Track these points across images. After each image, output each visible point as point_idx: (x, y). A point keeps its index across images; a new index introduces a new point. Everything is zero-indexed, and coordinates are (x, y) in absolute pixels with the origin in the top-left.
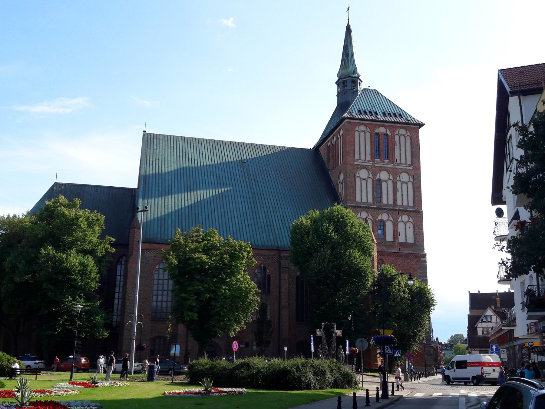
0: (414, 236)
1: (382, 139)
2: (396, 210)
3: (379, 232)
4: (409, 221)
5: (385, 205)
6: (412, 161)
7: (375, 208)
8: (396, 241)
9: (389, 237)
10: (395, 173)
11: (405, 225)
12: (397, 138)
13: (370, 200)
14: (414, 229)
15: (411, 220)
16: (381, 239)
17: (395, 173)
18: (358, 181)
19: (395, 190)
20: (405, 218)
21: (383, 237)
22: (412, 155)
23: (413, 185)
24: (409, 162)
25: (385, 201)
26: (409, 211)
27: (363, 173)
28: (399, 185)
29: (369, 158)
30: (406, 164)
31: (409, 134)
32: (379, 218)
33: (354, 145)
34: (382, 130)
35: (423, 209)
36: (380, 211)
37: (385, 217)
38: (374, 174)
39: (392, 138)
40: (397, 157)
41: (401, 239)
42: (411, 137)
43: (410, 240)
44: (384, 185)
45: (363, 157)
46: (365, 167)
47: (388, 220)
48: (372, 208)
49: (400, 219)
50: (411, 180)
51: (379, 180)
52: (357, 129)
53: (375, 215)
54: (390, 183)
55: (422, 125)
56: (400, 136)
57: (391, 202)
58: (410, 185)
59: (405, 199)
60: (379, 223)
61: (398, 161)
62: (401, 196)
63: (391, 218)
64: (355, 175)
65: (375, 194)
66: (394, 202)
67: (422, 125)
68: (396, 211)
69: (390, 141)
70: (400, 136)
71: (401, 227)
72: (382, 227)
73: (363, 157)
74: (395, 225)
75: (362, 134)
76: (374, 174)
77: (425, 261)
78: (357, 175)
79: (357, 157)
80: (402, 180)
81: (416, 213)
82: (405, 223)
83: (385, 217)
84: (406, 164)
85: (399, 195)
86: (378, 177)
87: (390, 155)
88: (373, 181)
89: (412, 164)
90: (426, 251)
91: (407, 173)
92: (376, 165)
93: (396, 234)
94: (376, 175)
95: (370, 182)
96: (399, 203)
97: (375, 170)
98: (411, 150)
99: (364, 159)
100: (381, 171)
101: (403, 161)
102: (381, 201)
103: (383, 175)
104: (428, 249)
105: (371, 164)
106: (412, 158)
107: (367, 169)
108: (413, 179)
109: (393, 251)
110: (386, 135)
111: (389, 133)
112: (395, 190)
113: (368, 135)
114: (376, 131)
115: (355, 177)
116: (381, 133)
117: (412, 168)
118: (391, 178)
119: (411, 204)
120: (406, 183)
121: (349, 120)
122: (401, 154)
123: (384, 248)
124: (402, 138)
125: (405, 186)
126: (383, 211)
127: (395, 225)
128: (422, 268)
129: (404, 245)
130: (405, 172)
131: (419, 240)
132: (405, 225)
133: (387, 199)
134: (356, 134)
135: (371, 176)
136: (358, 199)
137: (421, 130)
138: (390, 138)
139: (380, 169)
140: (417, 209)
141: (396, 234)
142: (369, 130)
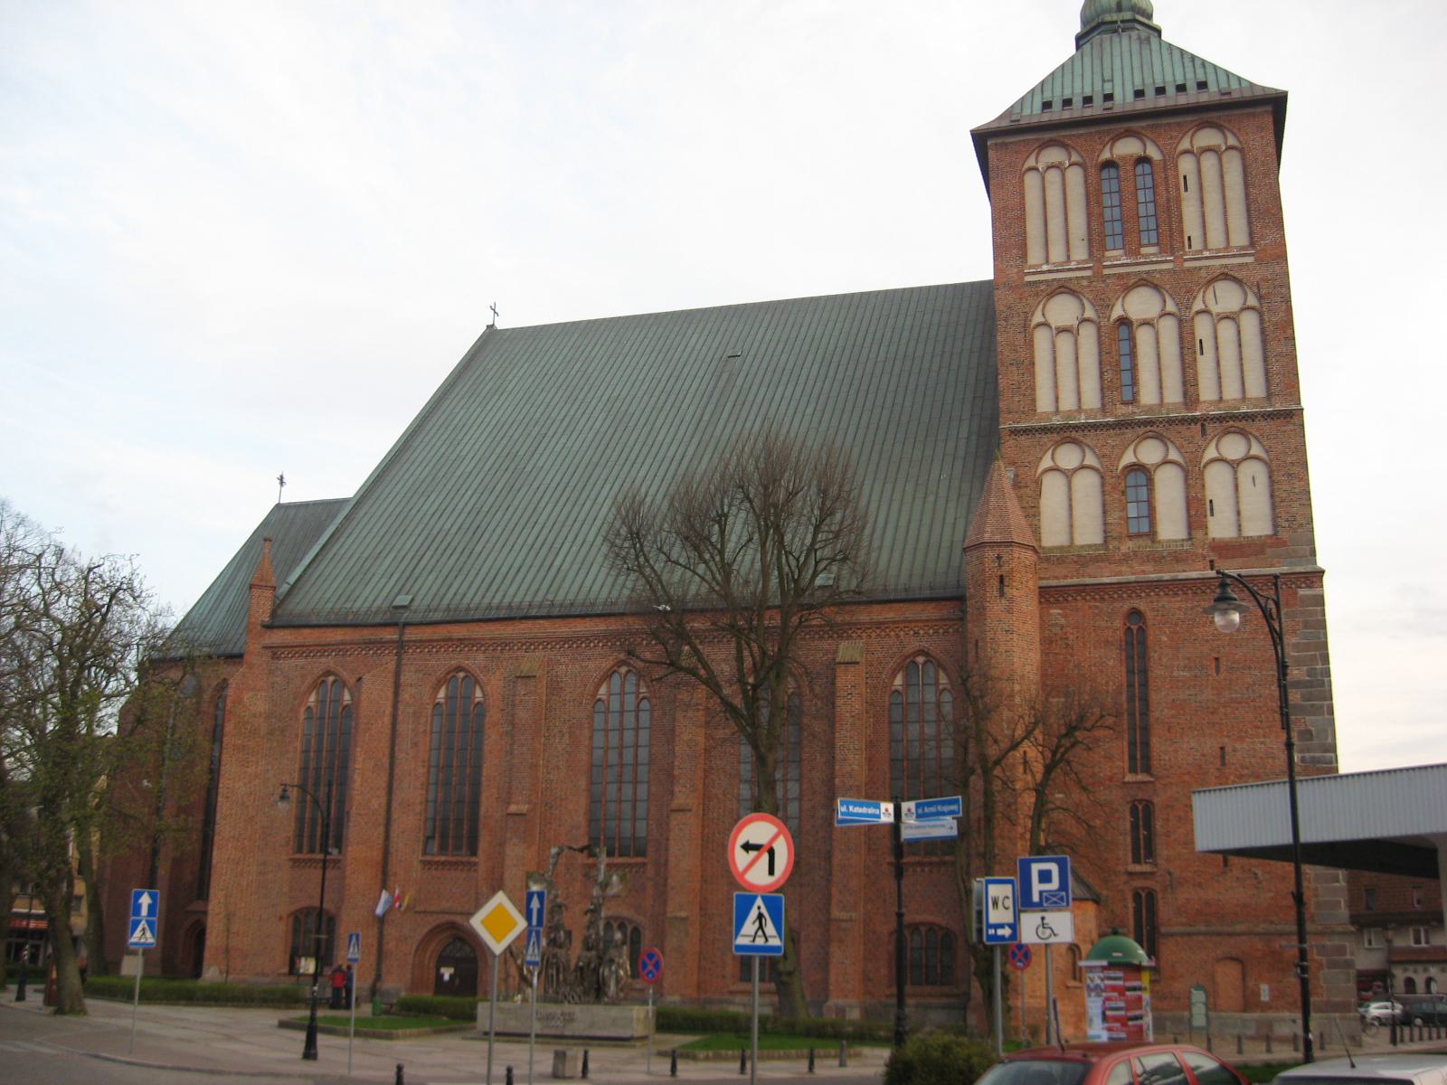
0: (1274, 507)
2: (1194, 420)
3: (1132, 511)
4: (1248, 458)
5: (1150, 409)
6: (1251, 234)
7: (1108, 426)
8: (1198, 534)
9: (1171, 527)
10: (1182, 288)
12: (1186, 165)
13: (1092, 399)
14: (1272, 481)
15: (1256, 450)
16: (1139, 535)
17: (1182, 288)
18: (1041, 339)
19: (1188, 348)
20: (1233, 447)
21: (1145, 528)
23: (1262, 321)
24: (1240, 238)
25: (1148, 396)
26: (1246, 417)
27: (1062, 310)
28: (1202, 328)
29: (1080, 253)
31: (1232, 141)
32: (1128, 458)
34: (1128, 148)
35: (1304, 404)
36: (1129, 433)
37: (1150, 452)
40: (1191, 226)
41: (1220, 527)
42: (1241, 151)
43: (1258, 525)
44: (1144, 337)
45: (1057, 254)
46: (1064, 288)
47: (1166, 462)
48: (1095, 427)
49: (1211, 453)
50: (1252, 301)
51: (1124, 321)
52: (1031, 162)
53: (1107, 451)
54: (1168, 328)
56: (1198, 154)
57: (1173, 395)
58: (1250, 323)
59: (1231, 376)
60: (1131, 480)
61: (1197, 245)
62: (1213, 365)
63: (1174, 455)
64: (1026, 321)
65: (1107, 376)
66: (1185, 394)
68: (1192, 426)
69: (1160, 177)
70: (1198, 154)
71: (1217, 483)
72: (1143, 493)
73: (1057, 254)
76: (1104, 305)
77: (1320, 601)
78: (1038, 318)
79: (1035, 256)
80: (1215, 309)
81: (1276, 422)
82: (1234, 465)
85: (1205, 364)
86: (1117, 312)
89: (1252, 244)
90: (1321, 562)
92: (1106, 272)
93: (1197, 510)
94: (1110, 307)
95: (1088, 335)
96: (1207, 392)
99: (1062, 258)
100: (1128, 289)
101: (1216, 240)
102: (1134, 400)
103: (1140, 304)
104: (1329, 550)
105: (1088, 273)
107: (1073, 292)
108: (1260, 298)
109: (1182, 575)
110: (1144, 160)
111: (1153, 153)
112: (1188, 348)
114: (1106, 155)
115: (1027, 330)
116: (1123, 158)
117: (1249, 260)
118: (1171, 307)
119: (1256, 388)
120: (1232, 317)
121: (1000, 140)
122: (1210, 216)
123: (1149, 567)
125: (1226, 330)
126: (1141, 431)
128: (1306, 625)
129: (1239, 548)
130: (1225, 276)
131: (1292, 519)
133: (1156, 386)
134: (1031, 181)
135: (1090, 313)
136: (1044, 403)
139: (1128, 285)
140: (1278, 407)
141: (1197, 510)
142: (1075, 158)
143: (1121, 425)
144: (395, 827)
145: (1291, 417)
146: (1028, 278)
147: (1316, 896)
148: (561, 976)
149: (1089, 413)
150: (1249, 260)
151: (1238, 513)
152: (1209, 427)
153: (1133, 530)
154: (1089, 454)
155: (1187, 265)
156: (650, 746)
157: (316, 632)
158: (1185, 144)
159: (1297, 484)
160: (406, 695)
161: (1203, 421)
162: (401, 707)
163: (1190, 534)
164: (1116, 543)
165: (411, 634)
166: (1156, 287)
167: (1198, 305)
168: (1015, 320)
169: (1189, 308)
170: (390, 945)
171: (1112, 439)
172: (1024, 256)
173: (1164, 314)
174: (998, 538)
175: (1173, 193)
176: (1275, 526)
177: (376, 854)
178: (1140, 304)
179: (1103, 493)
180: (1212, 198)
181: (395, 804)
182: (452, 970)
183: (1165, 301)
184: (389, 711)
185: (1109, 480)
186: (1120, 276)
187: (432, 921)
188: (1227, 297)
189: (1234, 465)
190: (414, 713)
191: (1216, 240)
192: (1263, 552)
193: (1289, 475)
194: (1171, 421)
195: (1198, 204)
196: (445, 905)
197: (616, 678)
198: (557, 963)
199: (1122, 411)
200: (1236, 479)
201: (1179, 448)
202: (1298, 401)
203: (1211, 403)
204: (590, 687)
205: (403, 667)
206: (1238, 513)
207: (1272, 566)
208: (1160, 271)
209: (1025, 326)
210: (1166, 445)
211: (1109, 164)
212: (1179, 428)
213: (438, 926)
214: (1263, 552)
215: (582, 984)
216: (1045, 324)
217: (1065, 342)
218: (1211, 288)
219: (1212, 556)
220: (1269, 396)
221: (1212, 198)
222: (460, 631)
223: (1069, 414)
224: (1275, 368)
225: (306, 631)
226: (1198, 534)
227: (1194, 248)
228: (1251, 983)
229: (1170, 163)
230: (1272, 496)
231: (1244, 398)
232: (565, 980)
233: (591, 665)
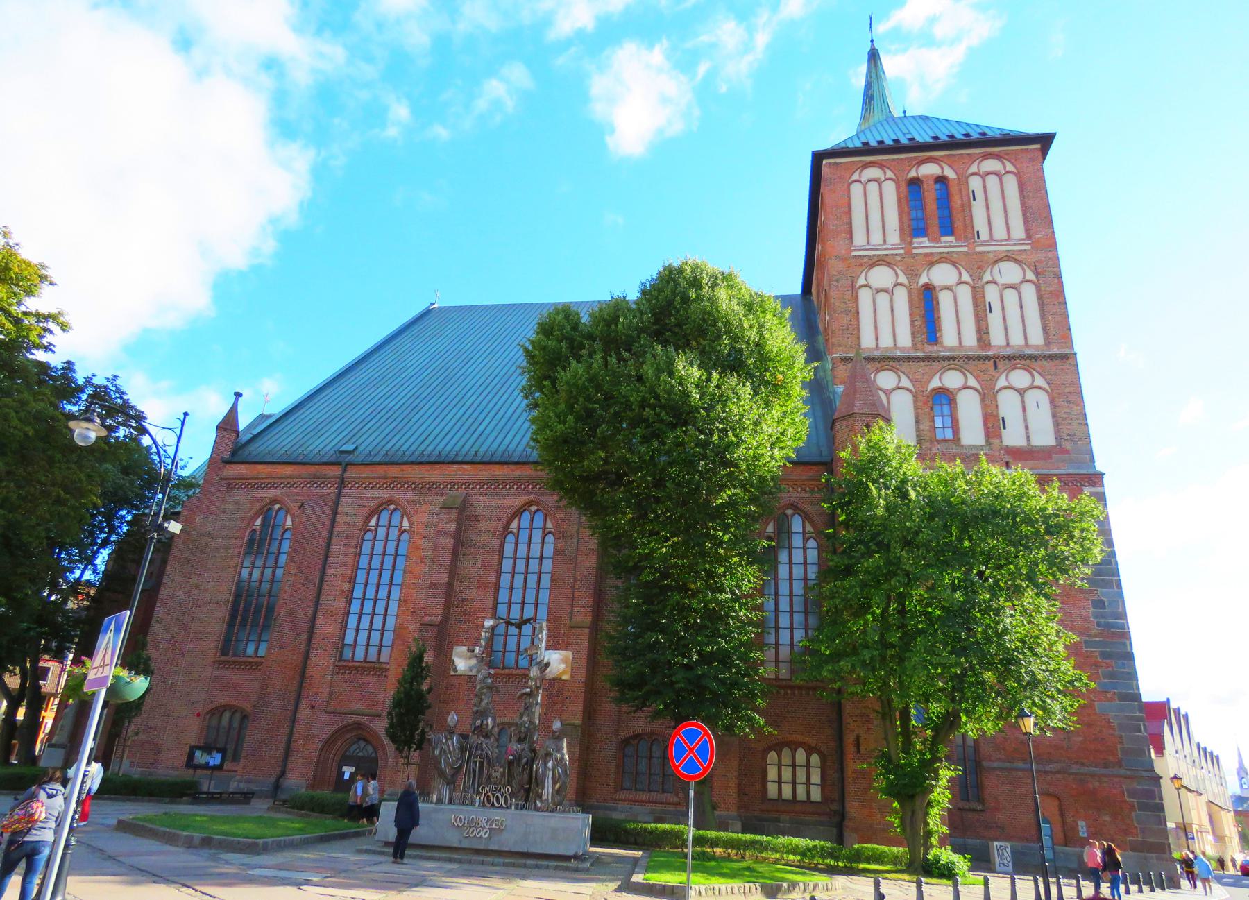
0: (1056, 424)
1: (931, 193)
2: (988, 358)
4: (1032, 387)
5: (952, 349)
6: (1027, 230)
8: (995, 442)
10: (977, 265)
11: (1022, 397)
12: (975, 183)
16: (946, 440)
17: (977, 265)
18: (865, 297)
19: (981, 309)
20: (1020, 378)
21: (949, 434)
22: (1024, 214)
23: (1038, 290)
24: (1018, 231)
25: (949, 338)
26: (1030, 357)
27: (881, 276)
28: (991, 294)
29: (894, 238)
30: (1009, 238)
32: (935, 383)
33: (849, 213)
35: (1077, 348)
36: (936, 365)
37: (952, 379)
38: (913, 274)
39: (959, 184)
40: (980, 224)
42: (1018, 175)
43: (1044, 436)
44: (945, 300)
45: (876, 239)
47: (965, 387)
48: (908, 359)
49: (1002, 382)
50: (1030, 275)
51: (929, 290)
52: (856, 176)
53: (918, 376)
54: (965, 294)
55: (1044, 141)
56: (984, 176)
57: (970, 339)
58: (1029, 293)
61: (984, 236)
66: (979, 339)
67: (1044, 141)
68: (988, 362)
70: (984, 176)
71: (1008, 405)
72: (946, 410)
73: (876, 239)
74: (988, 398)
75: (873, 187)
76: (913, 274)
78: (861, 281)
79: (859, 239)
80: (1001, 281)
81: (1055, 362)
82: (1021, 392)
83: (952, 379)
84: (1009, 238)
85: (994, 320)
86: (923, 280)
87: (958, 224)
88: (910, 292)
89: (1029, 237)
90: (1099, 466)
91: (1016, 261)
92: (915, 251)
94: (918, 276)
95: (901, 296)
96: (997, 338)
97: (911, 264)
98: (1023, 204)
100: (932, 264)
101: (1000, 233)
103: (941, 275)
105: (902, 252)
106: (1026, 222)
107: (889, 264)
108: (1037, 274)
111: (950, 173)
112: (981, 309)
113: (890, 189)
114: (913, 174)
115: (854, 289)
116: (927, 176)
117: (1029, 247)
118: (966, 277)
119: (1036, 338)
121: (832, 161)
124: (992, 181)
125: (1010, 296)
126: (946, 363)
127: (988, 398)
130: (1008, 257)
132: (1022, 397)
134: (856, 190)
135: (902, 279)
136: (867, 341)
137: (1053, 165)
138: (954, 189)
139: (931, 261)
140: (1055, 351)
143: (929, 359)
144: (318, 634)
145: (1067, 359)
146: (854, 254)
147: (1122, 743)
148: (485, 772)
149: (903, 349)
150: (1029, 247)
151: (1027, 428)
152: (1000, 364)
153: (939, 436)
154: (903, 377)
155: (978, 249)
156: (553, 572)
157: (269, 468)
158: (974, 169)
159: (1075, 408)
160: (341, 522)
161: (995, 360)
162: (336, 532)
163: (987, 441)
164: (928, 445)
165: (352, 472)
166: (954, 264)
167: (987, 277)
168: (844, 282)
169: (980, 278)
170: (298, 743)
171: (922, 367)
172: (851, 238)
173: (960, 283)
174: (866, 410)
175: (965, 201)
176: (1058, 438)
177: (297, 659)
178: (941, 275)
179: (916, 408)
180: (996, 205)
181: (320, 614)
182: (353, 769)
183: (960, 274)
184: (324, 533)
185: (920, 398)
186: (926, 255)
187: (339, 722)
188: (1010, 272)
189: (1021, 392)
190: (347, 537)
191: (1000, 233)
192: (1050, 458)
193: (1068, 401)
194: (969, 358)
195: (984, 209)
196: (354, 707)
197: (526, 516)
198: (481, 756)
199: (932, 350)
200: (1023, 402)
201: (977, 378)
202: (1072, 348)
203: (1000, 347)
204: (504, 521)
205: (342, 499)
206: (1027, 428)
207: (1058, 468)
208: (957, 253)
209: (853, 286)
210: (965, 375)
211: (915, 182)
212: (976, 362)
213: (345, 726)
214: (1050, 458)
215: (509, 783)
216: (867, 286)
217: (883, 299)
218: (996, 268)
219: (1007, 458)
220: (1048, 343)
221: (996, 205)
222: (393, 471)
223: (887, 349)
224: (1051, 324)
225: (260, 467)
226: (995, 442)
227: (982, 238)
228: (1069, 820)
229: (963, 179)
230: (1054, 416)
231: (1026, 344)
232: (489, 777)
233: (506, 503)
